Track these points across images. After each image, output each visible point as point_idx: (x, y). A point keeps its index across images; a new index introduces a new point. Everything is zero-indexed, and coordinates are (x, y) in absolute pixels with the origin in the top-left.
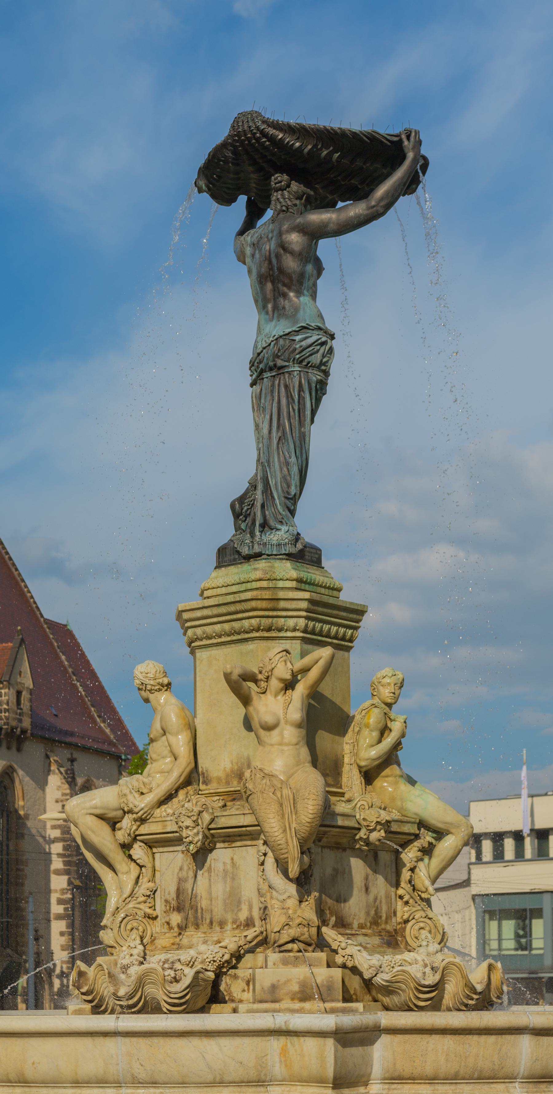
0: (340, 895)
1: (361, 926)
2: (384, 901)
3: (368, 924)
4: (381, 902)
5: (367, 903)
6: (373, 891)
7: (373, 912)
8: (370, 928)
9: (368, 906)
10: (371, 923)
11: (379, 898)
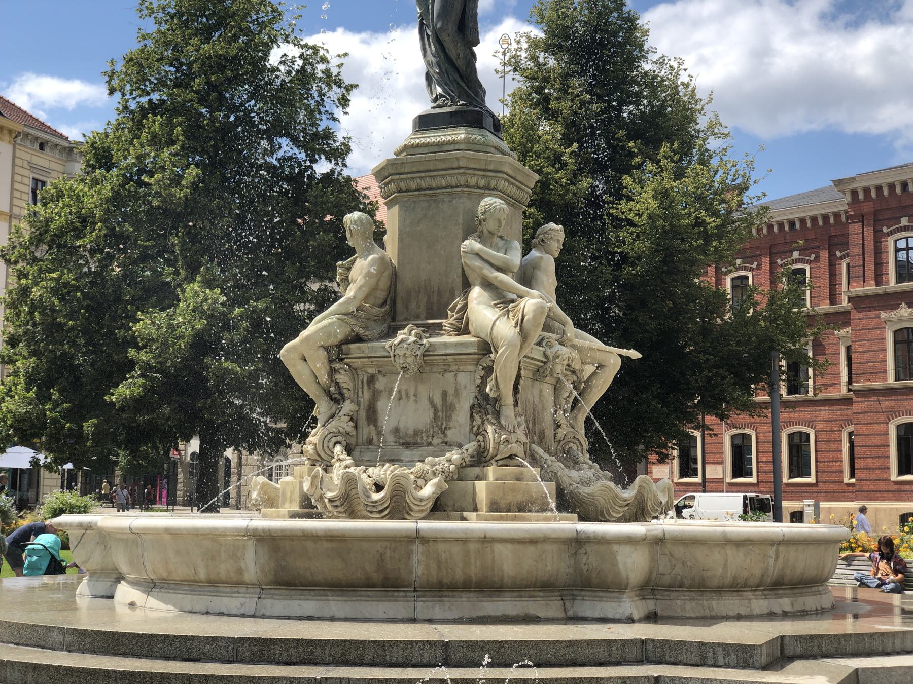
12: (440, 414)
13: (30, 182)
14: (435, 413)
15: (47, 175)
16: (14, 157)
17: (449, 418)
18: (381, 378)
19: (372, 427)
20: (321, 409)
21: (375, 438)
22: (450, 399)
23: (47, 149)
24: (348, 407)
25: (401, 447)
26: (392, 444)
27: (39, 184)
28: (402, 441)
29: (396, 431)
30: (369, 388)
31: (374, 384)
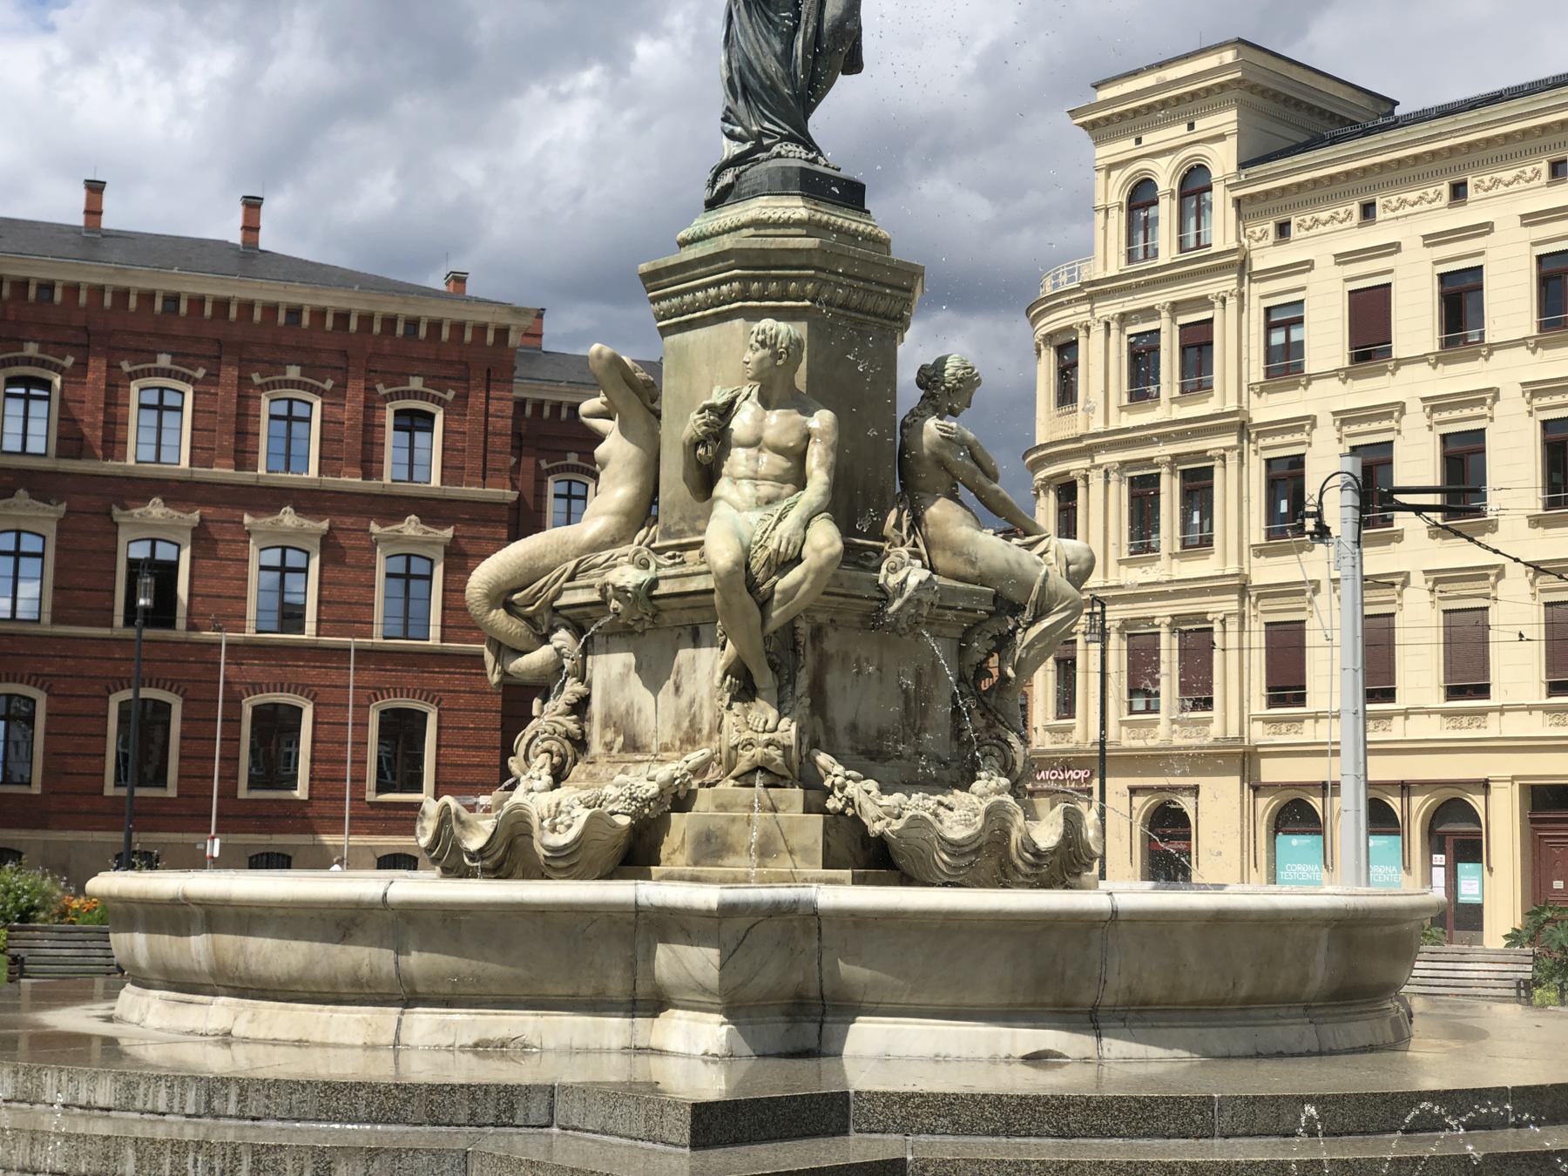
0: (632, 703)
1: (665, 748)
2: (706, 704)
3: (678, 743)
4: (701, 706)
5: (677, 709)
6: (688, 690)
7: (686, 724)
8: (681, 749)
9: (678, 716)
10: (682, 742)
11: (697, 700)
12: (913, 704)
14: (907, 703)
17: (924, 713)
18: (831, 633)
19: (818, 719)
21: (823, 738)
22: (925, 680)
25: (862, 757)
26: (847, 751)
28: (861, 747)
29: (853, 728)
30: (814, 648)
31: (822, 642)
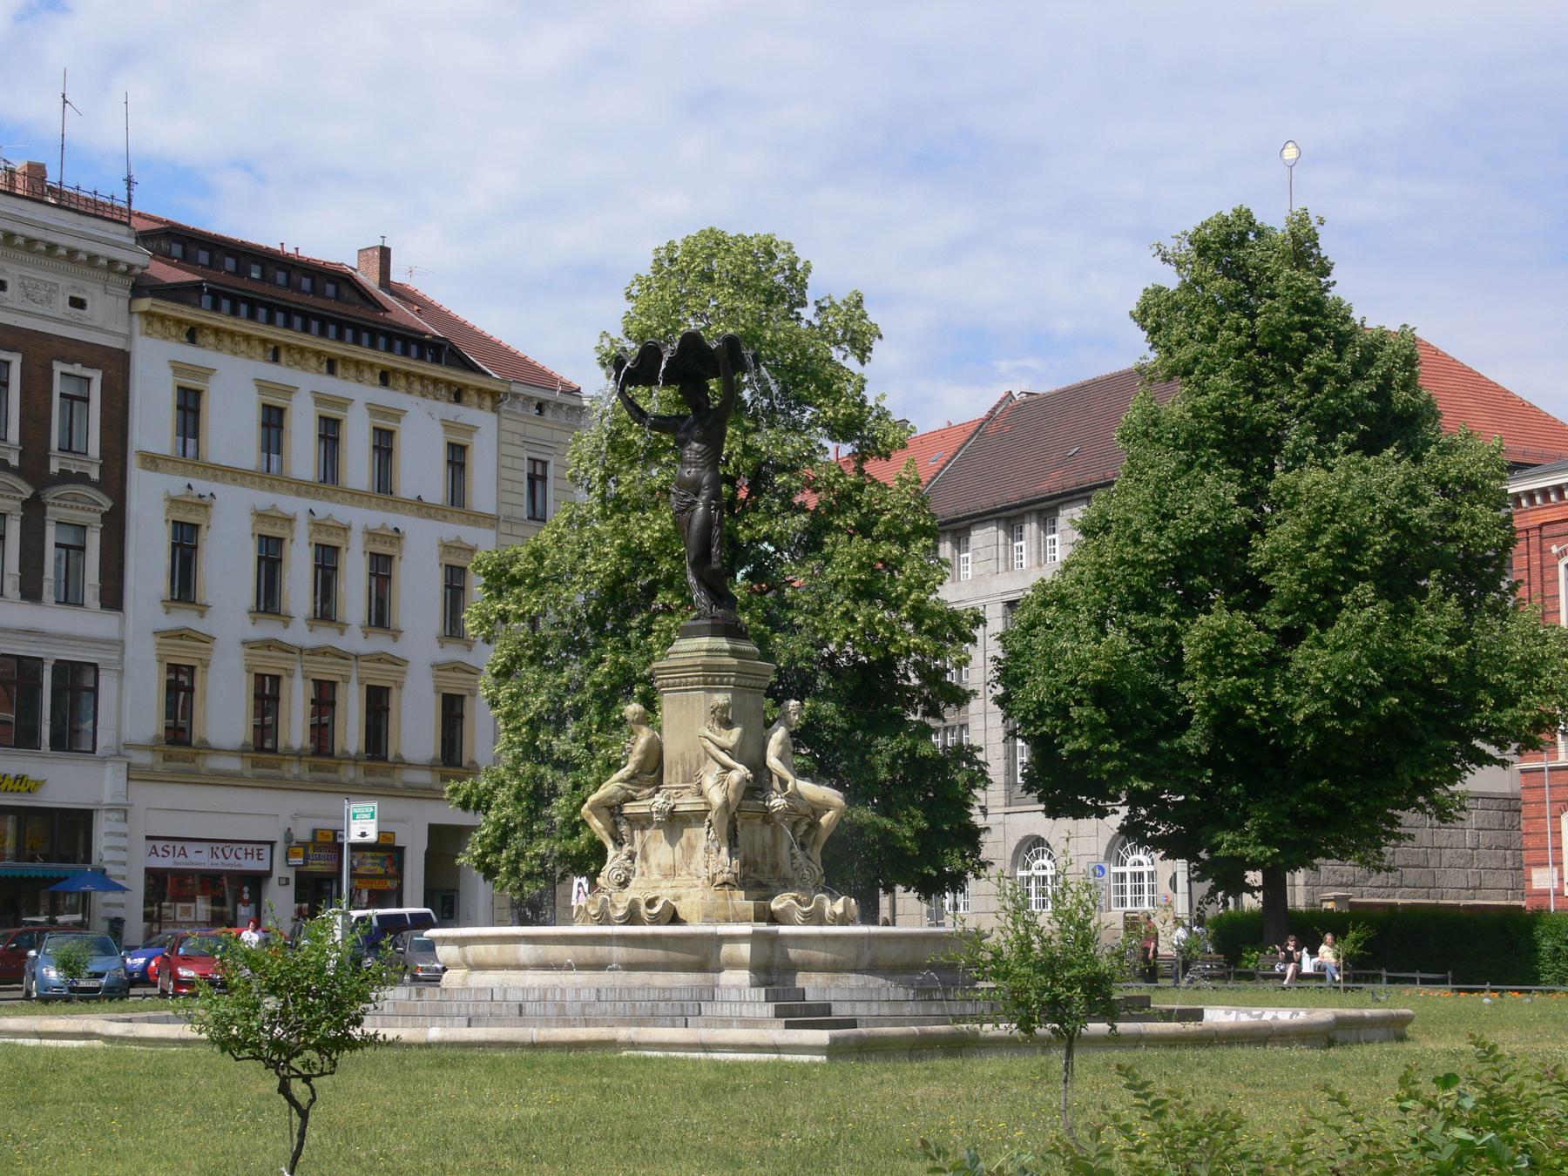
13: (525, 467)
15: (552, 452)
16: (500, 430)
20: (611, 852)
23: (548, 414)
24: (626, 848)
27: (539, 466)
